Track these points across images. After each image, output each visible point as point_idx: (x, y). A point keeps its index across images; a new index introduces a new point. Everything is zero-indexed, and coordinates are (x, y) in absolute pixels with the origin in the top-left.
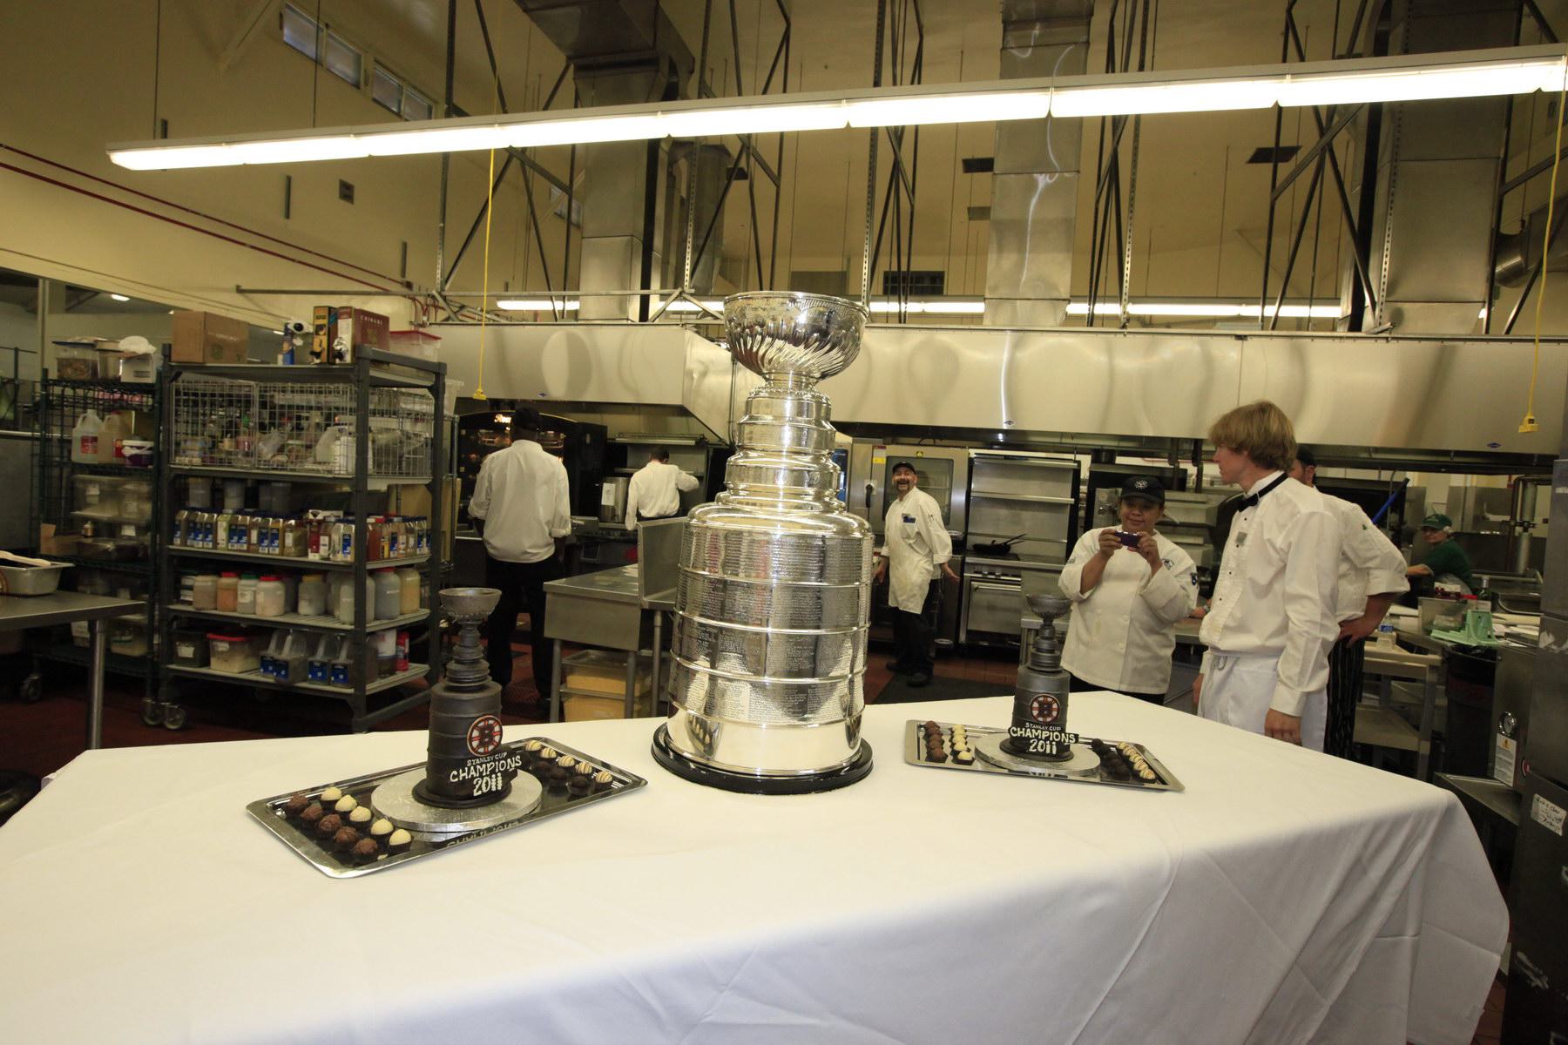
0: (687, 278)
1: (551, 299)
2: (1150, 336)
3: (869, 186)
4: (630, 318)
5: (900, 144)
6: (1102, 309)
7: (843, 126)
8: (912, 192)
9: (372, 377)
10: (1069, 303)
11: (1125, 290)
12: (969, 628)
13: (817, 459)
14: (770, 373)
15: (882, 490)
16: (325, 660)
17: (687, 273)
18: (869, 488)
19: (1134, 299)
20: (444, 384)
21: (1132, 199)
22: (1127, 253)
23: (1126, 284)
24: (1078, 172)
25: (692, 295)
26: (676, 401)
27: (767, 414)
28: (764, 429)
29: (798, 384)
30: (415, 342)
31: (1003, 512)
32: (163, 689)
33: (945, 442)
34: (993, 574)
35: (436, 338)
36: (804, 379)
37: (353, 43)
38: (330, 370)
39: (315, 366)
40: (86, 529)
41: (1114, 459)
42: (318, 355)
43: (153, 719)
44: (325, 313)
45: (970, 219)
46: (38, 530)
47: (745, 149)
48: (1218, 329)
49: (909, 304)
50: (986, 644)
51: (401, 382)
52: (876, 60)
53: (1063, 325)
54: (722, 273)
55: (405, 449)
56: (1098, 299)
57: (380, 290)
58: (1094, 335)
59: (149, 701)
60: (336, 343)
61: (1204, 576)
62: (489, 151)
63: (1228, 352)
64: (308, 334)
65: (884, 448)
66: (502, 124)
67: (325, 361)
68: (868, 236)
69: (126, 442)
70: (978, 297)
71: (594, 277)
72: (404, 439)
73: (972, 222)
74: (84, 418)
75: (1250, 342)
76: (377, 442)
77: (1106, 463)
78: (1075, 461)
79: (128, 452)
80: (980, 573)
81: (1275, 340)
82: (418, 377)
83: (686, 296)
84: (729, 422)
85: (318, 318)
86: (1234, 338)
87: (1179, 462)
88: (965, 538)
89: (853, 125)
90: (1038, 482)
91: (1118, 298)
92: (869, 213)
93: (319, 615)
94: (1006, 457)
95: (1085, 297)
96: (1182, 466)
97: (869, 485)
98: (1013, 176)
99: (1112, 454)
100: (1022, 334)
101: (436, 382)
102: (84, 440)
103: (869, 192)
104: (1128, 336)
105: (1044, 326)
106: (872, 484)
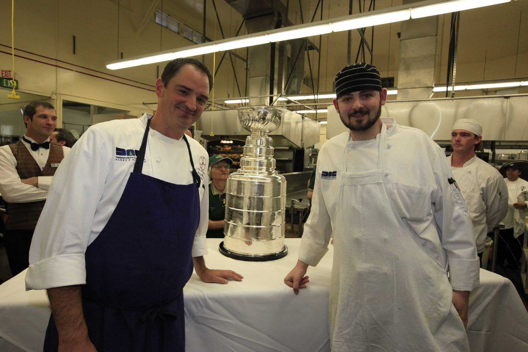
0: (283, 90)
1: (241, 99)
3: (348, 51)
4: (266, 104)
6: (450, 89)
7: (331, 32)
8: (371, 51)
17: (283, 88)
19: (457, 84)
25: (284, 96)
26: (280, 134)
28: (250, 149)
48: (497, 95)
52: (350, 3)
56: (449, 85)
58: (439, 101)
62: (214, 53)
63: (506, 102)
66: (216, 44)
71: (253, 92)
84: (302, 140)
86: (503, 98)
89: (335, 31)
92: (348, 61)
95: (445, 84)
103: (348, 53)
104: (454, 100)
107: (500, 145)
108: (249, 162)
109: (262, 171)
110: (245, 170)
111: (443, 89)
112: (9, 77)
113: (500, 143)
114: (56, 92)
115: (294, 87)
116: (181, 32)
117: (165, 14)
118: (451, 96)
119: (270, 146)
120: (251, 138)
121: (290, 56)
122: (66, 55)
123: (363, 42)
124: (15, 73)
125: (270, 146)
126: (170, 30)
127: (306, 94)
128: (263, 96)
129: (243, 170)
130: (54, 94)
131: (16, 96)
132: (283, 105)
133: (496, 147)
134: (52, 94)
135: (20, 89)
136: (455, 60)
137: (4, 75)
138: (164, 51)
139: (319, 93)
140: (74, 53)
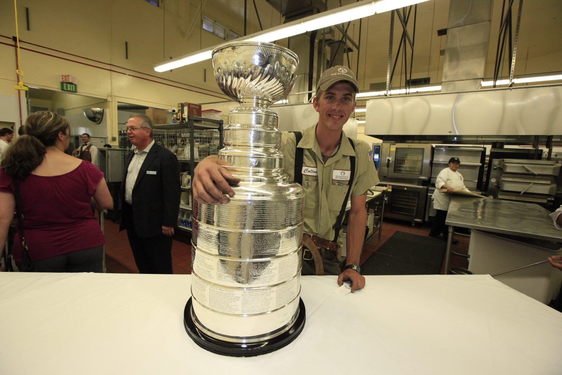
3: (390, 41)
5: (406, 23)
6: (499, 82)
7: (373, 14)
8: (412, 45)
9: (194, 126)
10: (483, 81)
11: (512, 69)
12: (430, 215)
13: (266, 150)
15: (394, 160)
16: (186, 219)
18: (389, 160)
21: (518, 26)
22: (514, 52)
23: (513, 67)
24: (490, 21)
27: (236, 123)
29: (257, 104)
30: (212, 113)
33: (423, 142)
37: (222, 25)
38: (182, 125)
39: (179, 124)
41: (503, 146)
42: (179, 119)
44: (180, 105)
47: (345, 37)
49: (410, 89)
51: (208, 127)
53: (480, 89)
55: (211, 150)
56: (498, 79)
57: (229, 100)
58: (494, 91)
60: (183, 115)
64: (177, 113)
65: (395, 144)
67: (181, 121)
68: (389, 61)
72: (210, 147)
73: (442, 56)
76: (199, 148)
77: (499, 148)
78: (483, 148)
82: (214, 125)
85: (179, 107)
90: (464, 157)
91: (507, 77)
93: (187, 204)
94: (449, 147)
95: (492, 78)
96: (540, 148)
99: (502, 144)
101: (220, 127)
103: (390, 44)
104: (513, 90)
105: (469, 90)
106: (390, 159)
111: (490, 83)
112: (68, 81)
114: (111, 95)
117: (212, 21)
118: (509, 85)
120: (237, 111)
121: (329, 59)
122: (119, 60)
123: (405, 34)
124: (74, 78)
126: (217, 35)
128: (301, 93)
130: (109, 96)
131: (24, 87)
134: (108, 97)
136: (516, 44)
137: (64, 80)
140: (127, 58)
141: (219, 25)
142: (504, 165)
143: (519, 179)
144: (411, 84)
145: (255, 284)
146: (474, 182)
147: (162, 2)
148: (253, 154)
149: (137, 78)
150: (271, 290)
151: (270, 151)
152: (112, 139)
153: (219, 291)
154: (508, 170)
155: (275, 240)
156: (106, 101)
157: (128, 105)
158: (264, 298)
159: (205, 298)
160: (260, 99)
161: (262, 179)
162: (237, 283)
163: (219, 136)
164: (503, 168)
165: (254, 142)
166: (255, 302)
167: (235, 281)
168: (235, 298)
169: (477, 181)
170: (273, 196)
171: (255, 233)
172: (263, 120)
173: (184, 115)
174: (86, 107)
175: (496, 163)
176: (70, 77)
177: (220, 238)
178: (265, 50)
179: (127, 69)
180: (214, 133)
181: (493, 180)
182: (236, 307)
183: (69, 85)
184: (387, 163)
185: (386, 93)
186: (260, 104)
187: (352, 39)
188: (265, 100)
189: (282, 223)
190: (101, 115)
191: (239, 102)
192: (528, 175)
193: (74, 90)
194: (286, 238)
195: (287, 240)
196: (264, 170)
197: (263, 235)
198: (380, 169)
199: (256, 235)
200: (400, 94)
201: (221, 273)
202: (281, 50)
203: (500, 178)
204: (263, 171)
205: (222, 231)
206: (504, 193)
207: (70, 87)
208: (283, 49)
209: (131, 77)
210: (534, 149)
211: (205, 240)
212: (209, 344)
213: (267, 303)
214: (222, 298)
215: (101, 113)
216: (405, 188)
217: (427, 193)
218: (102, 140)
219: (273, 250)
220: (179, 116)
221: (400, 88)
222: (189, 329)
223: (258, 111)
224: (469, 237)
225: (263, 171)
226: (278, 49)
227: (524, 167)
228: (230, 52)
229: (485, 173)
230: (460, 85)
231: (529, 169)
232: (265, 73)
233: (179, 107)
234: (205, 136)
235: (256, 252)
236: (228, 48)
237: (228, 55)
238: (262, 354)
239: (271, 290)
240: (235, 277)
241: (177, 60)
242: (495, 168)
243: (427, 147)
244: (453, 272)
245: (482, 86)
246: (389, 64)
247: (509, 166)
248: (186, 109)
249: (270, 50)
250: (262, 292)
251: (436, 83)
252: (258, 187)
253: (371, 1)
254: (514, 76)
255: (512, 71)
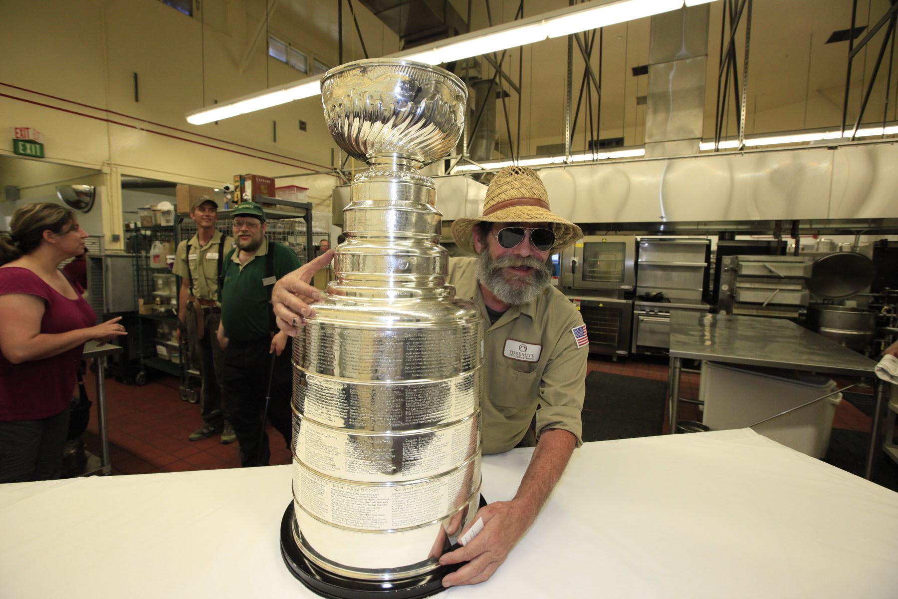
0: (465, 148)
2: (762, 154)
3: (568, 81)
5: (589, 55)
6: (723, 145)
7: (544, 38)
8: (599, 88)
10: (702, 141)
12: (638, 344)
13: (419, 243)
14: (370, 158)
15: (582, 261)
18: (574, 262)
20: (311, 214)
21: (746, 64)
22: (743, 100)
23: (743, 122)
24: (707, 55)
29: (400, 166)
30: (293, 192)
31: (659, 273)
32: (187, 382)
33: (621, 232)
34: (653, 311)
35: (306, 189)
36: (406, 160)
37: (303, 52)
40: (157, 301)
41: (734, 237)
43: (185, 396)
44: (238, 179)
45: (638, 103)
46: (138, 301)
47: (498, 74)
49: (599, 154)
50: (649, 354)
54: (496, 148)
57: (314, 172)
58: (720, 157)
59: (182, 388)
60: (244, 195)
61: (801, 310)
69: (169, 257)
70: (642, 145)
73: (640, 107)
74: (155, 246)
75: (839, 150)
77: (728, 240)
78: (707, 240)
79: (169, 261)
80: (644, 310)
81: (860, 147)
82: (296, 212)
83: (465, 159)
85: (236, 182)
86: (826, 149)
87: (782, 237)
88: (635, 290)
94: (661, 239)
95: (712, 138)
96: (784, 239)
97: (574, 260)
98: (662, 65)
99: (733, 234)
100: (669, 161)
101: (307, 214)
102: (157, 257)
104: (745, 155)
106: (575, 260)
107: (811, 229)
108: (361, 258)
109: (403, 286)
110: (347, 284)
111: (710, 146)
112: (27, 139)
113: (811, 225)
114: (109, 162)
115: (481, 152)
116: (310, 71)
117: (284, 43)
119: (428, 206)
121: (474, 108)
122: (123, 103)
123: (588, 73)
124: (38, 133)
125: (428, 206)
126: (293, 67)
127: (501, 159)
129: (340, 283)
130: (106, 165)
132: (466, 173)
133: (800, 232)
134: (103, 165)
135: (53, 158)
136: (745, 90)
138: (274, 88)
139: (521, 157)
140: (137, 100)
141: (295, 49)
142: (739, 264)
143: (760, 284)
144: (599, 147)
145: (410, 474)
146: (697, 291)
147: (198, 9)
148: (395, 251)
149: (156, 135)
150: (440, 482)
151: (425, 244)
152: (111, 239)
153: (350, 491)
154: (744, 272)
155: (444, 395)
156: (99, 172)
157: (139, 180)
158: (430, 496)
159: (324, 506)
160: (405, 158)
161: (413, 293)
162: (382, 474)
163: (305, 229)
164: (736, 269)
165: (400, 230)
166: (415, 505)
167: (378, 472)
168: (379, 501)
169: (702, 290)
170: (432, 320)
171: (411, 385)
172: (412, 192)
173: (246, 195)
174: (63, 184)
175: (727, 261)
176: (31, 132)
177: (350, 397)
178: (418, 75)
179: (134, 118)
180: (296, 224)
181: (725, 288)
182: (382, 517)
183: (28, 145)
184: (571, 267)
185: (565, 160)
186: (405, 167)
187: (508, 76)
188: (413, 160)
189: (455, 366)
190: (90, 197)
191: (369, 164)
192: (772, 278)
193: (39, 154)
194: (461, 391)
195: (462, 394)
196: (416, 278)
197: (422, 388)
198: (561, 276)
199: (412, 389)
200: (585, 161)
201: (353, 459)
202: (444, 76)
203: (734, 284)
204: (414, 280)
205: (353, 385)
206: (740, 305)
207: (31, 149)
208: (448, 74)
209: (144, 132)
210: (777, 240)
211: (321, 404)
212: (338, 589)
213: (434, 505)
214: (357, 503)
215: (91, 193)
216: (599, 304)
217: (633, 310)
218: (94, 240)
219: (442, 412)
220: (237, 197)
221: (584, 152)
222: (294, 564)
223: (405, 178)
224: (699, 374)
225: (414, 280)
226: (439, 74)
227: (765, 267)
228: (358, 77)
229: (712, 277)
230: (671, 148)
231: (773, 269)
232: (419, 111)
233: (236, 182)
234: (281, 230)
235: (414, 419)
236: (354, 71)
237: (354, 81)
238: (430, 596)
239: (440, 482)
240: (379, 465)
241: (227, 105)
242: (726, 269)
243: (630, 240)
244: (682, 428)
245: (701, 149)
246: (567, 115)
247: (746, 266)
248: (248, 185)
249: (427, 75)
250: (425, 487)
251: (633, 144)
252: (402, 307)
253: (540, 19)
254: (745, 135)
255: (742, 128)
